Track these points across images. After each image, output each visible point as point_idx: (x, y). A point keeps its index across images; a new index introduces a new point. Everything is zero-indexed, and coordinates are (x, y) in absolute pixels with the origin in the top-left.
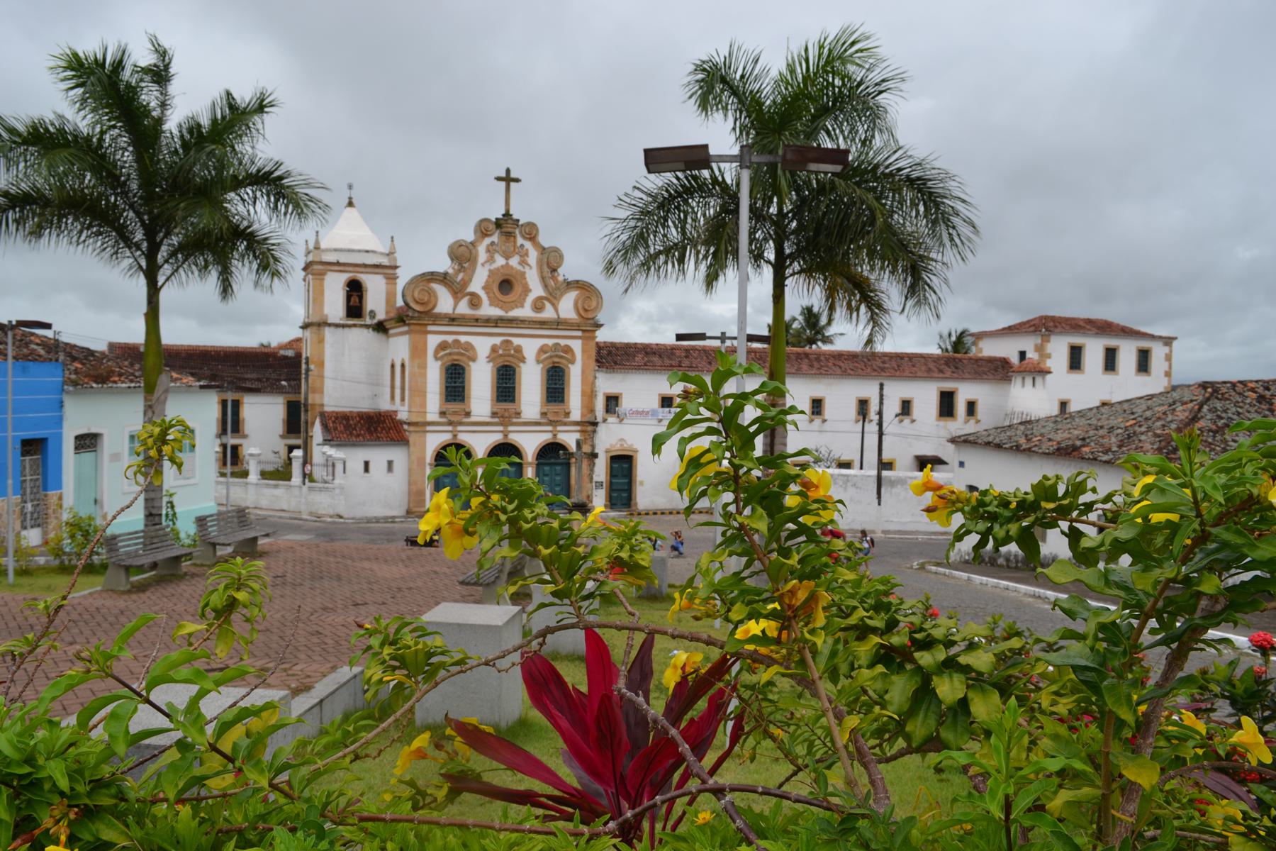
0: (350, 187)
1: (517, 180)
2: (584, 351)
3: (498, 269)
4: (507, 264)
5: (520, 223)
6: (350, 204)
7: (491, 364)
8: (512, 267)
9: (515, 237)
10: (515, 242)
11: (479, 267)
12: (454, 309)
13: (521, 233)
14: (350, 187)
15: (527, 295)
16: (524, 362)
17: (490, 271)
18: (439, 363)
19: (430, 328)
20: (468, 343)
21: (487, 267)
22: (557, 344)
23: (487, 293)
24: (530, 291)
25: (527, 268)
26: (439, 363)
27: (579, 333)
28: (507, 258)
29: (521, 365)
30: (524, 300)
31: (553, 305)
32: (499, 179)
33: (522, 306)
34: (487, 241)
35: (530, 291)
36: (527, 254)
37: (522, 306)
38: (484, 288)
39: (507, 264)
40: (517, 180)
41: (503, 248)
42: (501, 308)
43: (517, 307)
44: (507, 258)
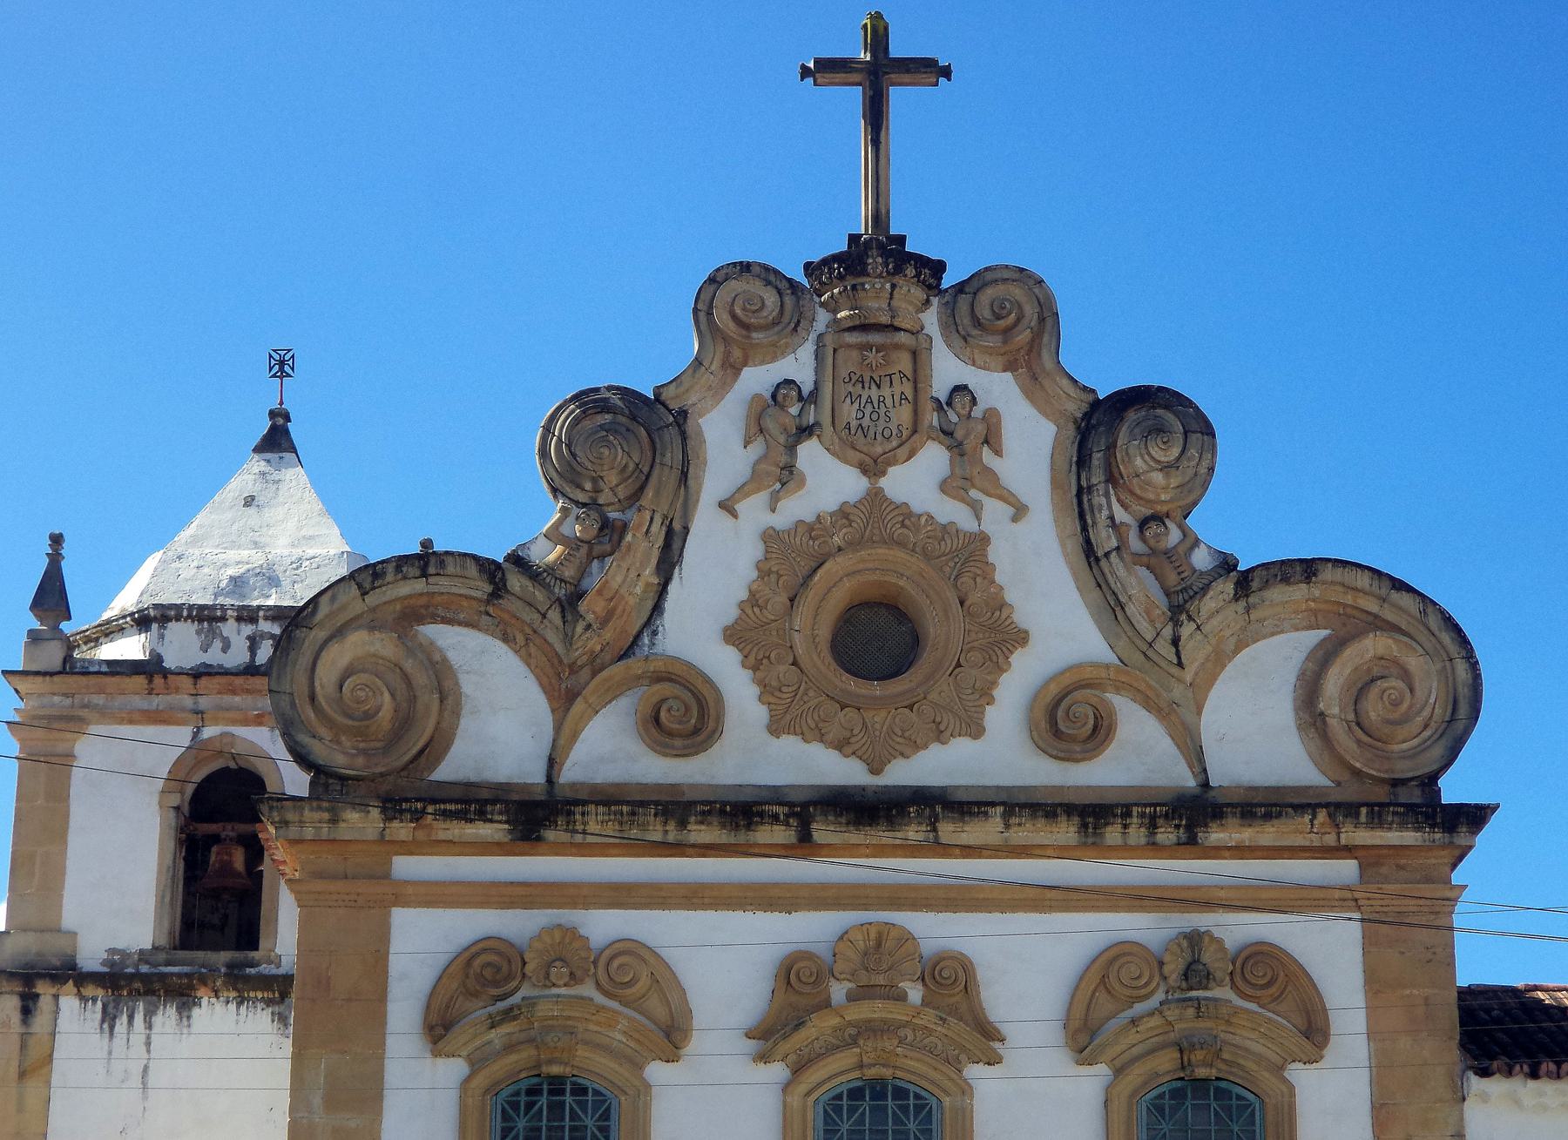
0: (281, 366)
1: (930, 70)
2: (1375, 982)
3: (812, 529)
4: (875, 498)
5: (948, 280)
6: (277, 440)
7: (777, 1071)
8: (906, 515)
9: (919, 356)
10: (918, 376)
11: (705, 524)
12: (553, 763)
13: (950, 324)
14: (281, 366)
15: (1000, 668)
16: (993, 1060)
17: (770, 537)
18: (452, 1070)
19: (406, 866)
20: (631, 950)
21: (755, 512)
22: (1194, 939)
23: (755, 664)
24: (1022, 638)
25: (995, 511)
26: (452, 1070)
27: (1345, 870)
28: (873, 468)
29: (975, 1072)
30: (986, 695)
31: (1164, 711)
32: (828, 69)
33: (975, 729)
34: (757, 379)
35: (1022, 638)
36: (992, 439)
37: (975, 729)
38: (732, 635)
39: (875, 498)
40: (930, 70)
41: (849, 412)
42: (841, 746)
43: (940, 735)
44: (873, 468)
